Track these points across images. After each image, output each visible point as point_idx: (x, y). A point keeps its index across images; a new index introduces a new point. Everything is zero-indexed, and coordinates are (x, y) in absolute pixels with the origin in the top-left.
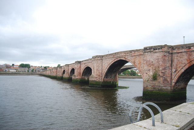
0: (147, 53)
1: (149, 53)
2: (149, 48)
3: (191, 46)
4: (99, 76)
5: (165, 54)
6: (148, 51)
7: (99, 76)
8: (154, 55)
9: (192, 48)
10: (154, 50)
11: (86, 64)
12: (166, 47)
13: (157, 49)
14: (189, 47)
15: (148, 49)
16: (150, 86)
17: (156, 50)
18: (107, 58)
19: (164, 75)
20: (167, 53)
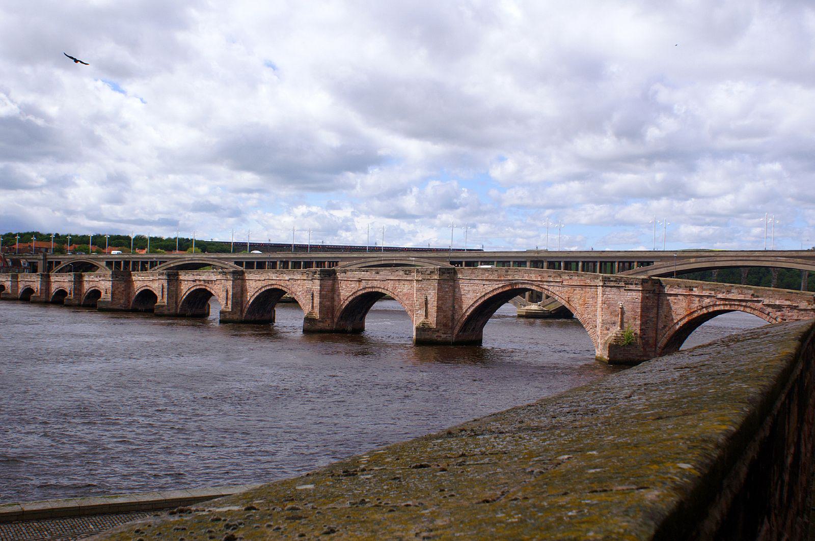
0: (609, 289)
1: (614, 290)
2: (614, 279)
3: (693, 287)
4: (445, 325)
5: (648, 295)
6: (612, 284)
7: (445, 325)
8: (626, 294)
9: (694, 289)
10: (625, 284)
11: (363, 284)
12: (650, 282)
13: (632, 284)
14: (690, 287)
15: (612, 281)
16: (620, 354)
17: (630, 286)
18: (473, 277)
19: (645, 335)
20: (652, 292)
